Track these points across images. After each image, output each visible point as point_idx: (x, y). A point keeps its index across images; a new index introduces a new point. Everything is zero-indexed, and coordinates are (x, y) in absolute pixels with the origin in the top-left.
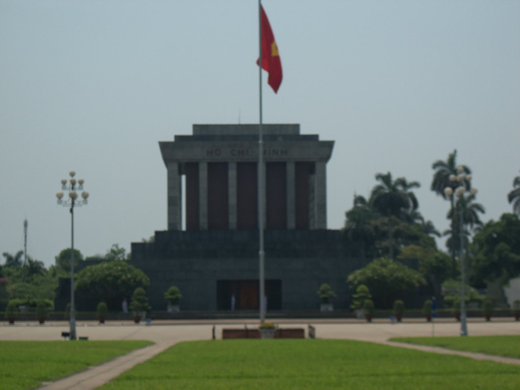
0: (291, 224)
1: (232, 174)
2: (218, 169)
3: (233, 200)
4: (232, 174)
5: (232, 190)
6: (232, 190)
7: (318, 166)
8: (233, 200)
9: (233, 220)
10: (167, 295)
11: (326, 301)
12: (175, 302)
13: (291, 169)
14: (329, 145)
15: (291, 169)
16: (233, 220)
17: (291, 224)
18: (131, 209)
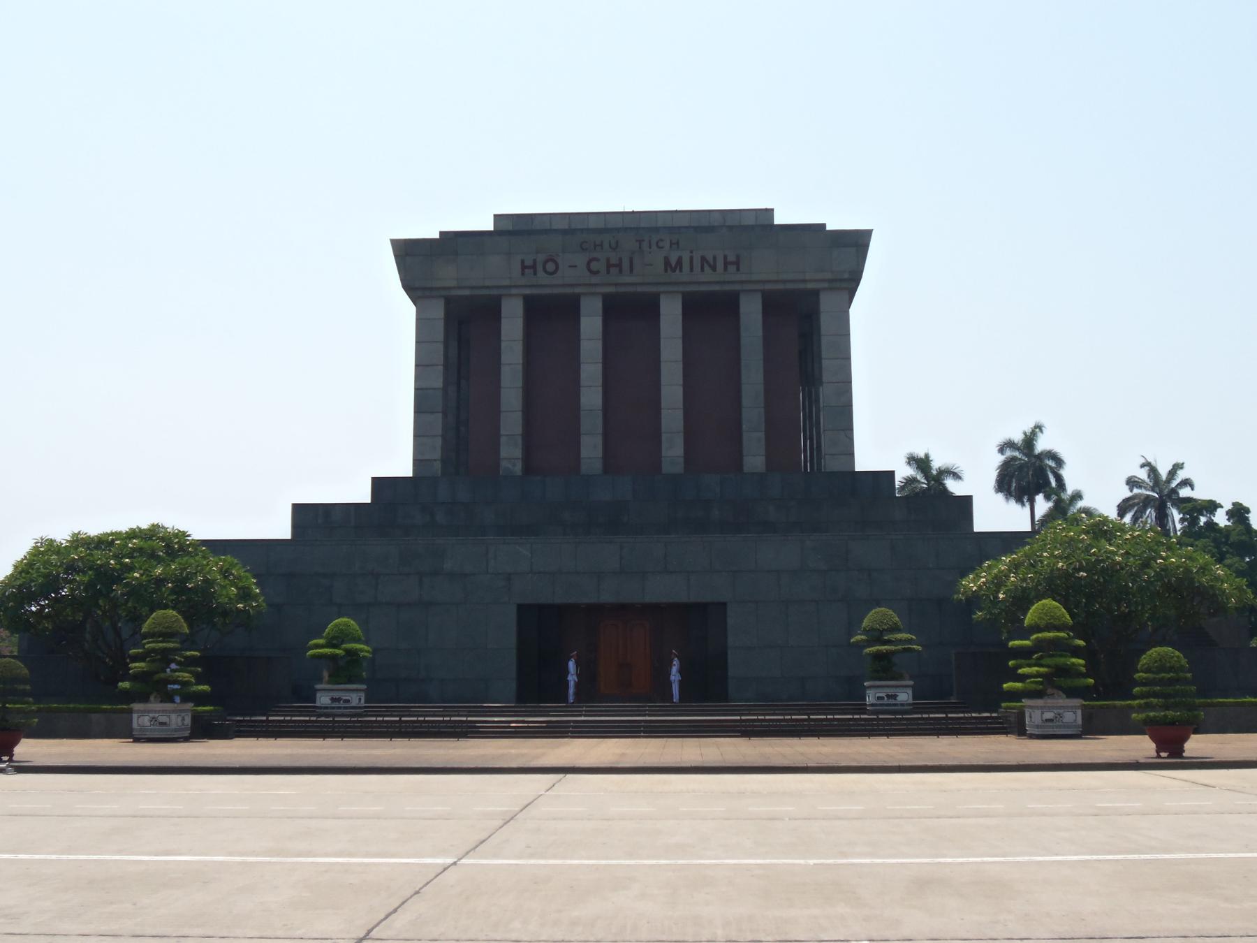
0: (754, 460)
1: (591, 325)
2: (551, 316)
3: (591, 397)
4: (591, 325)
5: (591, 371)
6: (591, 371)
7: (827, 303)
8: (591, 397)
9: (591, 449)
10: (318, 647)
11: (884, 667)
12: (345, 669)
13: (751, 311)
14: (854, 245)
15: (751, 311)
16: (591, 449)
17: (754, 460)
18: (305, 418)
